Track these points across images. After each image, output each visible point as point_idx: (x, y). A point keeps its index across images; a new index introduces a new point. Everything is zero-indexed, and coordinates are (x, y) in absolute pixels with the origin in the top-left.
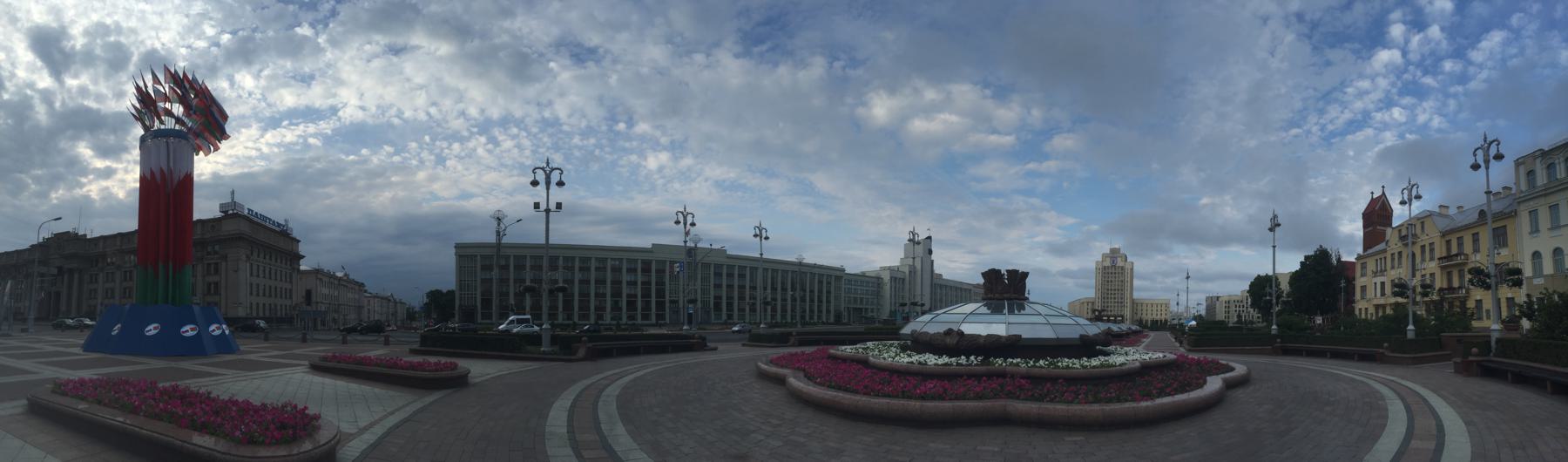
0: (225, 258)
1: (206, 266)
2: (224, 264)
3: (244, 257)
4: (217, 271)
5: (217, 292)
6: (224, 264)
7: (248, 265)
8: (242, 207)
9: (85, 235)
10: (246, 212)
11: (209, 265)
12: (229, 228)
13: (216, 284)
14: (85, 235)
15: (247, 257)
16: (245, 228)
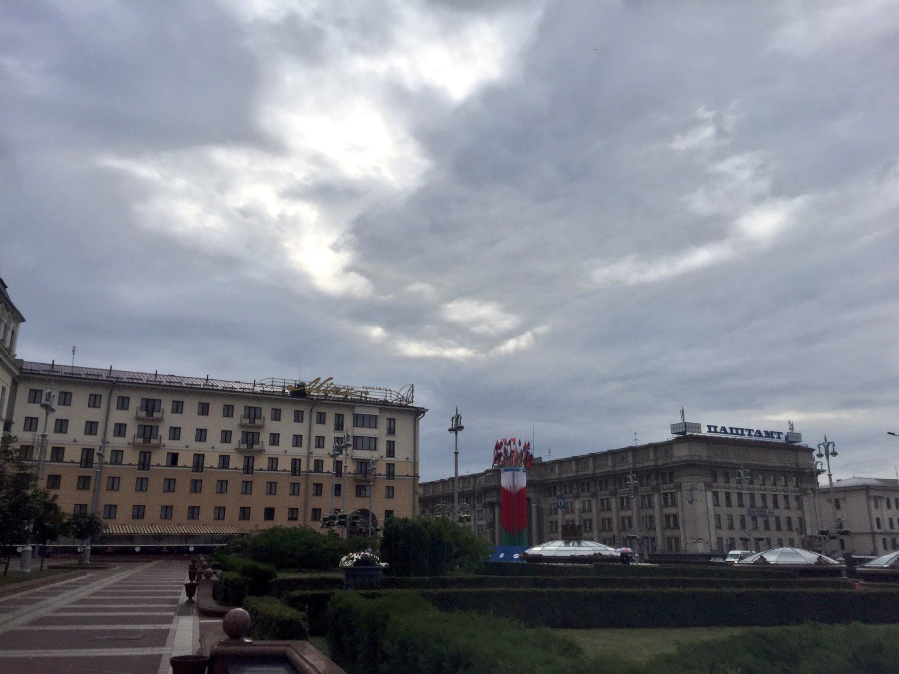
0: (679, 487)
1: (662, 496)
2: (679, 493)
3: (701, 486)
4: (674, 504)
5: (676, 526)
6: (679, 493)
7: (709, 494)
8: (698, 427)
9: (540, 459)
10: (704, 431)
11: (666, 494)
12: (682, 453)
13: (675, 517)
14: (540, 459)
15: (708, 486)
16: (701, 453)
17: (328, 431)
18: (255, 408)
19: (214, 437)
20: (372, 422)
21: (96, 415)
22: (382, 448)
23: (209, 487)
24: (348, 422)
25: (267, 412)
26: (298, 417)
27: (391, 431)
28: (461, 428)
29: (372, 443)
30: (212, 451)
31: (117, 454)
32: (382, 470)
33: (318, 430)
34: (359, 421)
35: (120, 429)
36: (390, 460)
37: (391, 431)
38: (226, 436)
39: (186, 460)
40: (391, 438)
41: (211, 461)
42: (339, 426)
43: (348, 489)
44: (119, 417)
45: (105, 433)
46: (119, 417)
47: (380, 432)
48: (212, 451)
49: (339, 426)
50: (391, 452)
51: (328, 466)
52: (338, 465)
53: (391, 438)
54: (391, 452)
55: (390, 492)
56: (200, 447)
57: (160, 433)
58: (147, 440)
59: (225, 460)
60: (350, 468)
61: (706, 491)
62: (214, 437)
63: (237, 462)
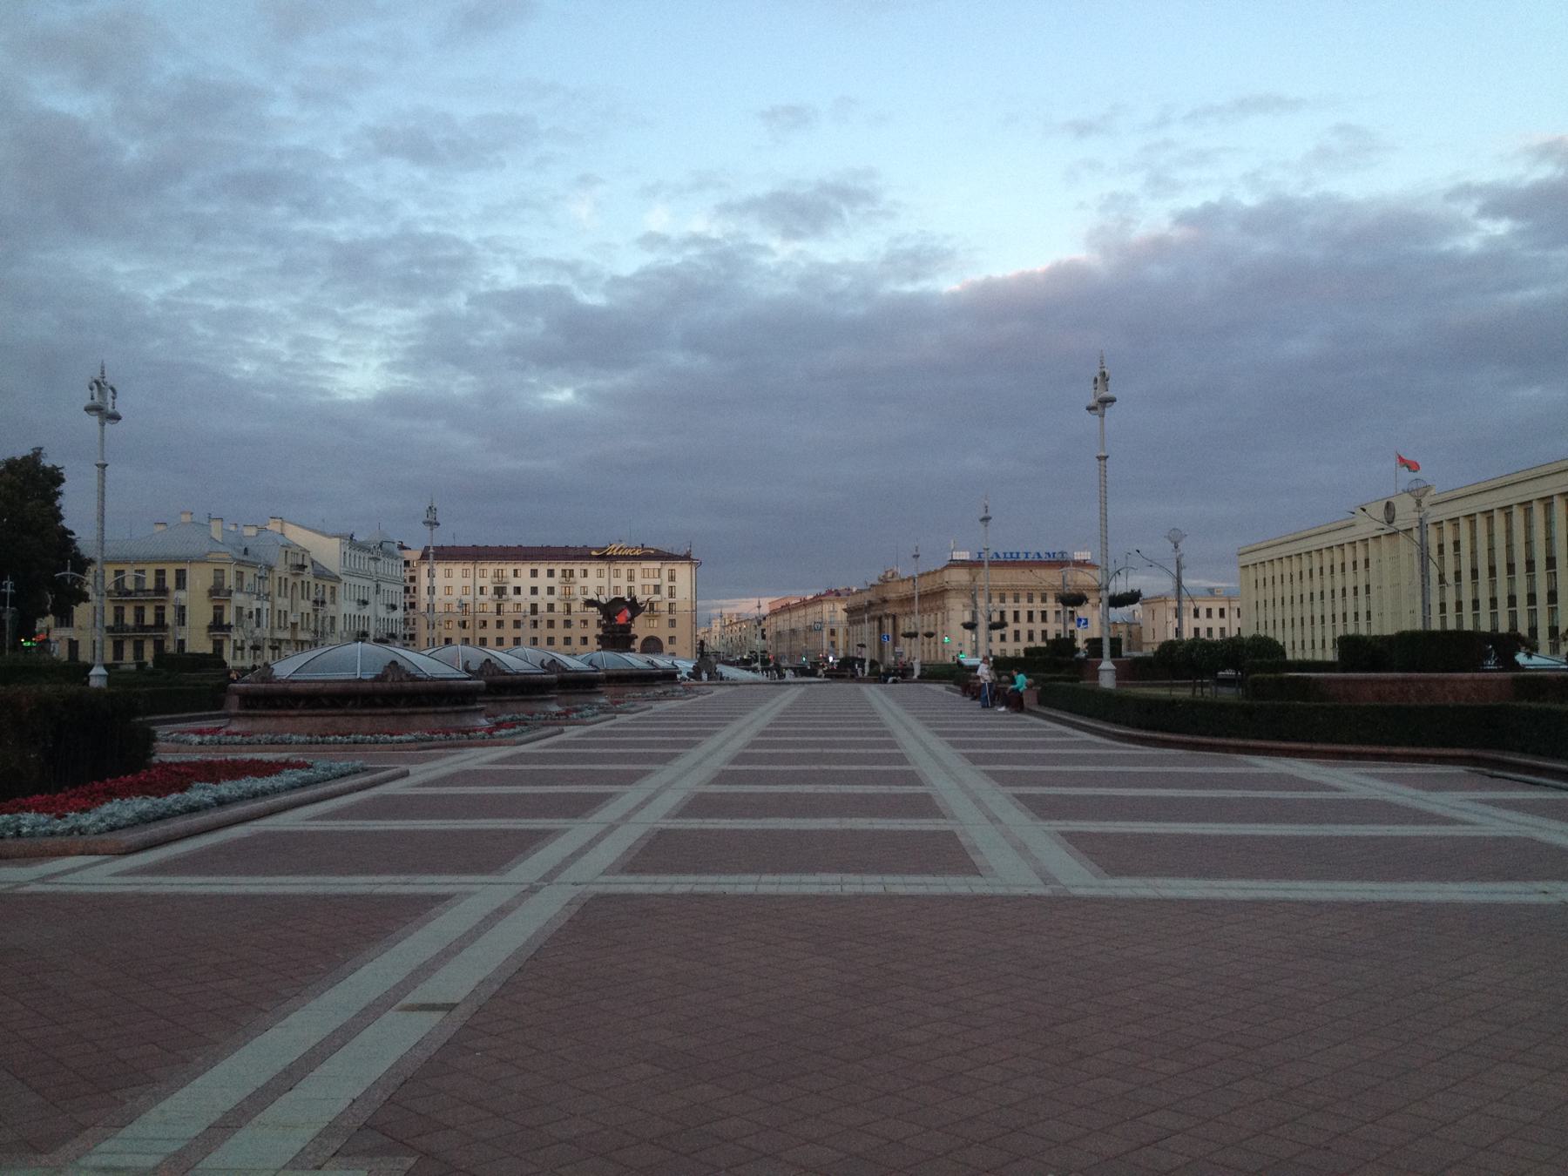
19: (543, 591)
23: (543, 626)
25: (577, 573)
27: (672, 578)
30: (542, 599)
32: (664, 607)
36: (672, 600)
37: (672, 578)
38: (551, 590)
40: (672, 584)
41: (542, 607)
42: (631, 578)
45: (475, 594)
48: (542, 599)
49: (631, 578)
50: (671, 595)
53: (672, 584)
54: (671, 595)
56: (534, 599)
57: (508, 591)
58: (500, 597)
59: (551, 607)
61: (963, 611)
62: (543, 591)
63: (559, 607)
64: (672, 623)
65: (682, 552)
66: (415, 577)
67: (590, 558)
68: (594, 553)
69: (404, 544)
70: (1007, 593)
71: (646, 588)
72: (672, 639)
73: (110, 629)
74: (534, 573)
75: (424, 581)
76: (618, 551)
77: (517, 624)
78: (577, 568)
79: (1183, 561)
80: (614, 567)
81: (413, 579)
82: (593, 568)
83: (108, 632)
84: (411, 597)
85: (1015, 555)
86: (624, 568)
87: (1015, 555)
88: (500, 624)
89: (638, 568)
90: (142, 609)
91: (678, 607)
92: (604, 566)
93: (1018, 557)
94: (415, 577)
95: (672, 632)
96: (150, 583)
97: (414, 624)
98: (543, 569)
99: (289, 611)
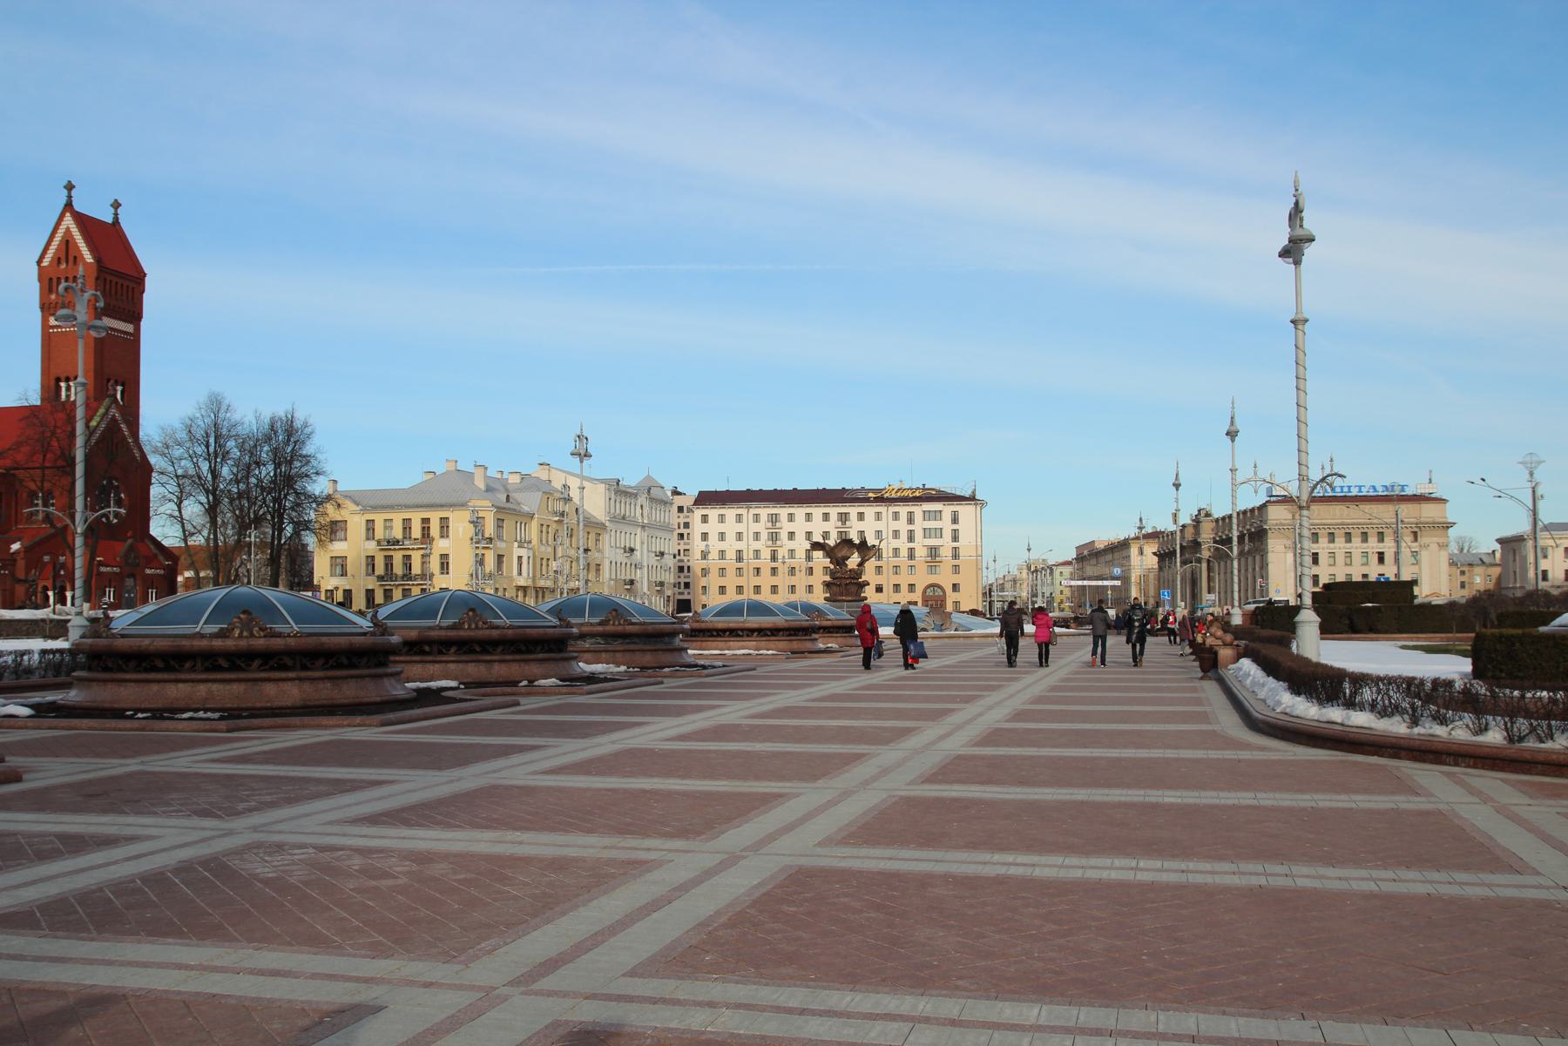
17: (903, 525)
18: (846, 513)
20: (937, 515)
21: (741, 527)
22: (948, 535)
24: (918, 516)
26: (878, 516)
27: (955, 520)
28: (587, 455)
29: (939, 533)
31: (757, 552)
33: (895, 525)
34: (927, 515)
35: (757, 536)
37: (955, 520)
39: (731, 555)
40: (955, 527)
42: (911, 521)
43: (922, 568)
44: (755, 527)
46: (755, 527)
47: (946, 524)
49: (911, 521)
50: (955, 538)
51: (904, 553)
52: (911, 550)
53: (955, 527)
54: (955, 538)
55: (956, 569)
60: (921, 553)
64: (956, 569)
65: (967, 494)
66: (688, 523)
67: (867, 500)
68: (871, 495)
69: (679, 490)
70: (1370, 532)
71: (927, 531)
72: (955, 587)
73: (380, 578)
74: (809, 517)
75: (698, 527)
76: (896, 492)
77: (792, 571)
78: (853, 510)
79: (1539, 492)
80: (893, 509)
81: (687, 525)
82: (870, 511)
83: (378, 581)
84: (685, 544)
85: (1345, 489)
86: (903, 510)
87: (1345, 489)
88: (774, 571)
89: (918, 510)
90: (409, 557)
91: (962, 553)
92: (882, 509)
93: (1350, 492)
94: (688, 523)
95: (955, 579)
96: (416, 532)
97: (689, 571)
98: (817, 511)
99: (552, 558)
